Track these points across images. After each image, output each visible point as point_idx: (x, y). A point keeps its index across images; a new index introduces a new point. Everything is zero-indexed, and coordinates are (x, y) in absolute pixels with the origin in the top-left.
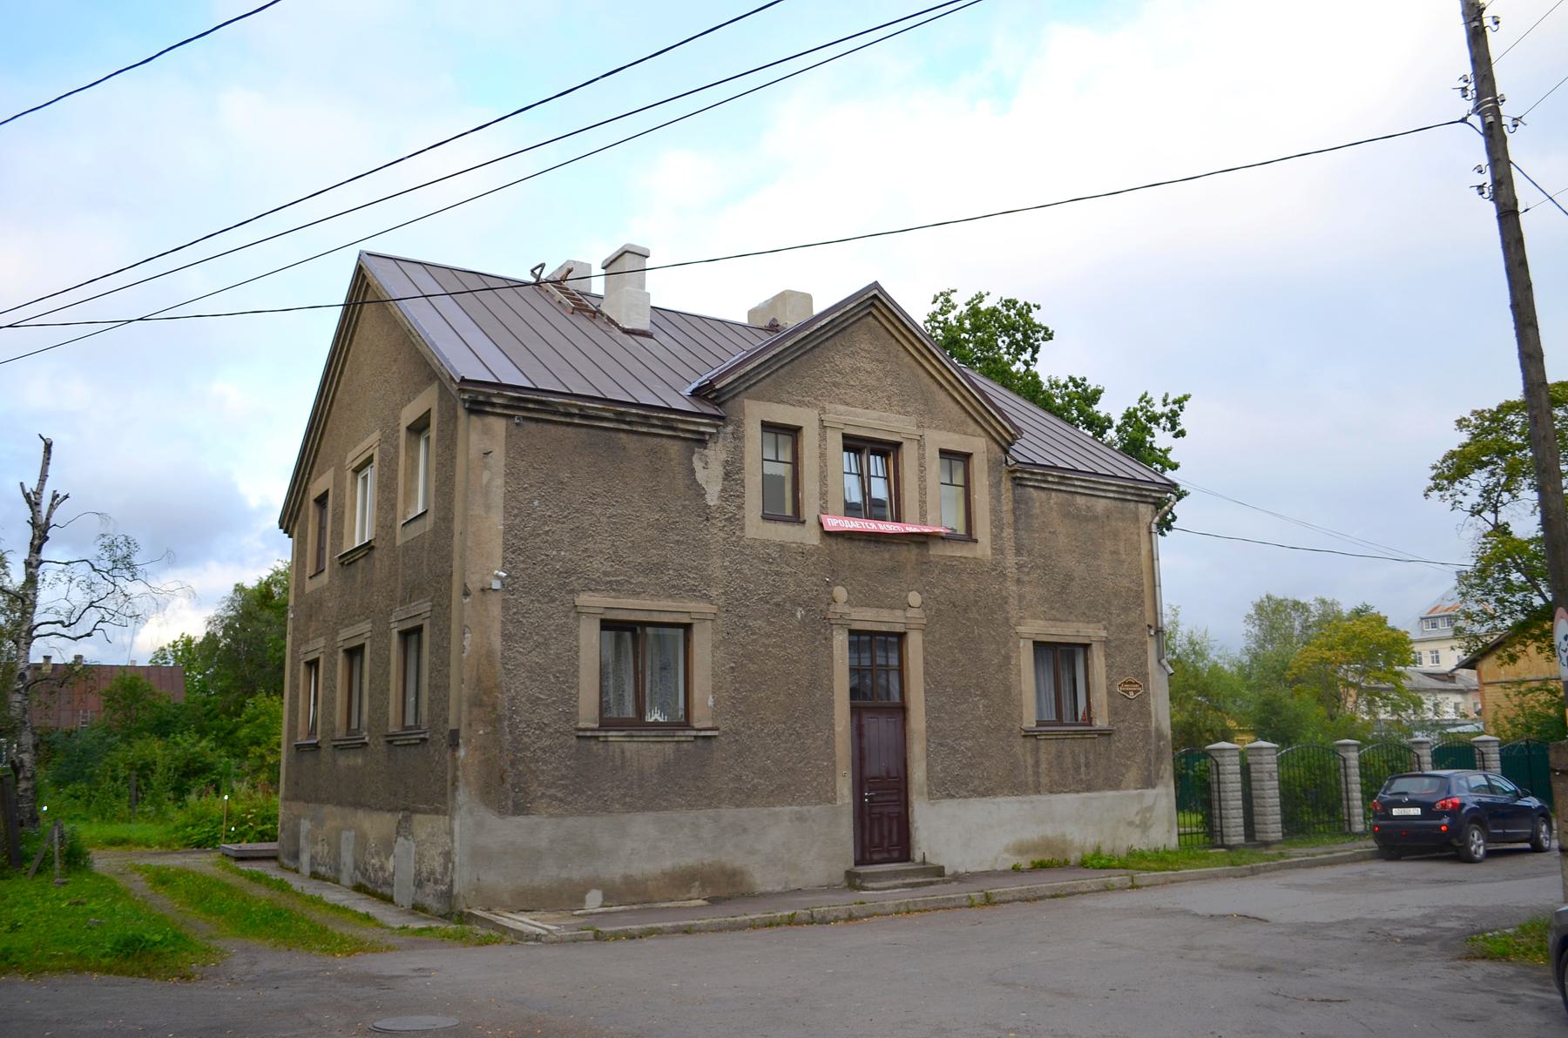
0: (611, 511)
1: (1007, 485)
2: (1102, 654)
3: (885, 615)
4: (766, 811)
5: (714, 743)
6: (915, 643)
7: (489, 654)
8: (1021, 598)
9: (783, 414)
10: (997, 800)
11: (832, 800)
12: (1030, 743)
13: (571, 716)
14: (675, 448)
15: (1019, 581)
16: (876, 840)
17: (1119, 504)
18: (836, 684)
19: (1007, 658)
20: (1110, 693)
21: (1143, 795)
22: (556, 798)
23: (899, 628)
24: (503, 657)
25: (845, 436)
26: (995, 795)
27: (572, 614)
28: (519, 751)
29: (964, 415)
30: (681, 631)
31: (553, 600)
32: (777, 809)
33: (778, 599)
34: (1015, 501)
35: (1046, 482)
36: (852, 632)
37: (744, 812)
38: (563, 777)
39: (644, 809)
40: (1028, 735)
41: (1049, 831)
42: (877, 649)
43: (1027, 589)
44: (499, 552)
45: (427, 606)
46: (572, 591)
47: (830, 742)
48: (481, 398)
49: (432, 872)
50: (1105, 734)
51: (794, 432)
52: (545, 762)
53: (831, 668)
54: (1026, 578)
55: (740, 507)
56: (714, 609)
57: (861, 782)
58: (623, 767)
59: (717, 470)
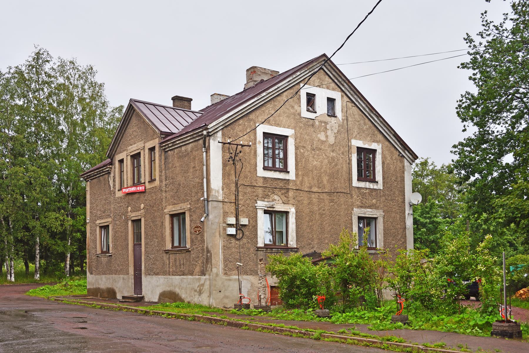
1: (163, 153)
15: (166, 191)
19: (162, 222)
20: (191, 233)
21: (200, 279)
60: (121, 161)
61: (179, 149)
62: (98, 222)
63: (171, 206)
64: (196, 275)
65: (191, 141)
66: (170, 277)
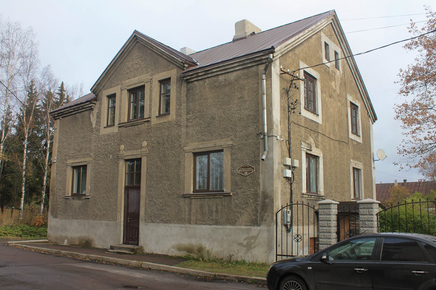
3: (135, 152)
4: (99, 222)
6: (144, 161)
8: (187, 133)
10: (171, 225)
12: (187, 201)
13: (64, 193)
15: (187, 126)
19: (179, 162)
20: (232, 174)
21: (249, 230)
23: (139, 157)
25: (128, 90)
26: (171, 223)
34: (188, 90)
36: (126, 160)
38: (63, 209)
39: (75, 219)
40: (185, 196)
42: (134, 165)
54: (191, 124)
55: (99, 126)
57: (127, 214)
60: (112, 97)
61: (215, 78)
62: (70, 162)
63: (196, 143)
65: (238, 68)
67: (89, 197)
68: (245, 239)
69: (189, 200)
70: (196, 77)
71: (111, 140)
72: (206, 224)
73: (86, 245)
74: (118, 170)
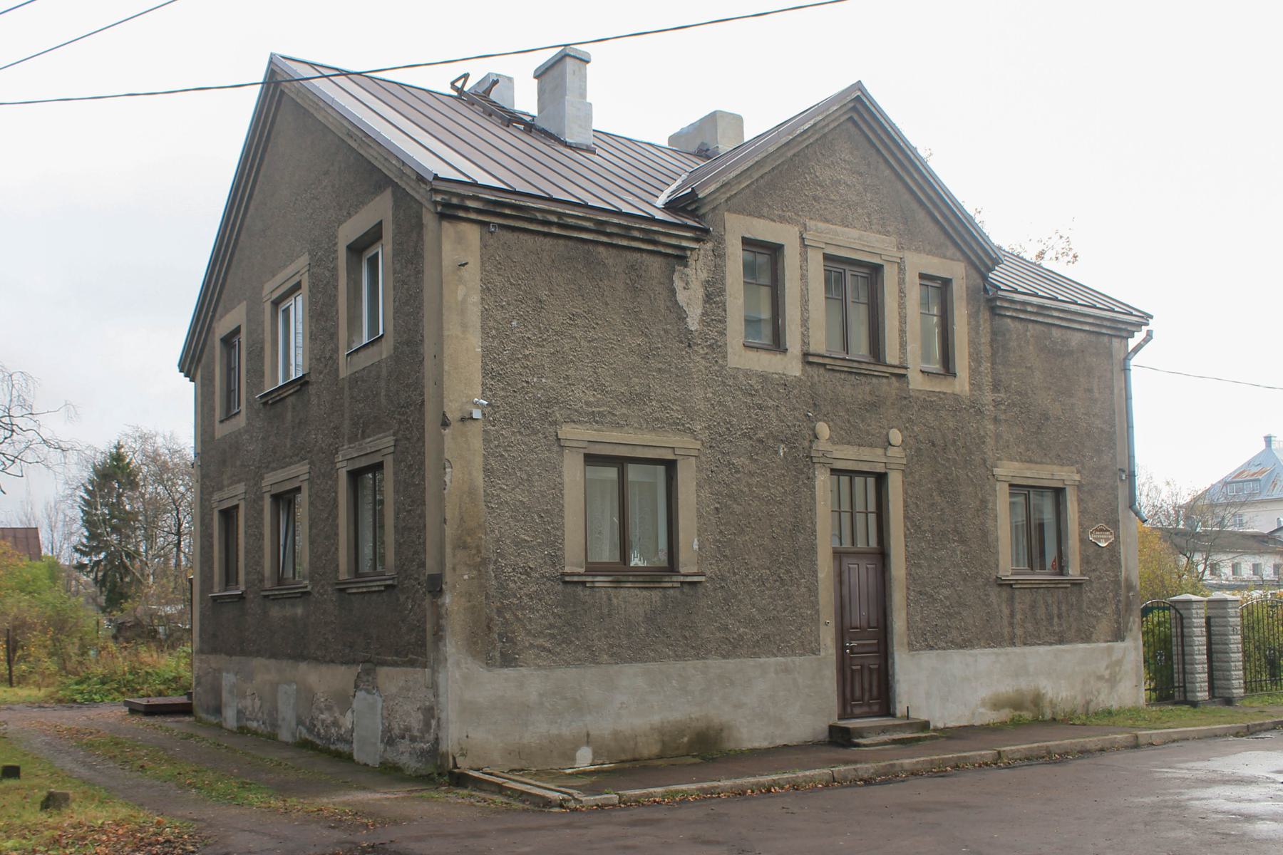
0: (592, 334)
1: (985, 315)
2: (1075, 498)
4: (751, 662)
5: (701, 590)
6: (895, 483)
7: (472, 492)
8: (998, 437)
9: (765, 230)
11: (816, 651)
13: (556, 559)
14: (655, 264)
16: (858, 693)
17: (1093, 338)
18: (819, 527)
19: (984, 502)
21: (1110, 651)
22: (545, 649)
24: (487, 495)
26: (973, 647)
27: (556, 448)
28: (506, 597)
29: (942, 238)
30: (661, 469)
31: (536, 432)
32: (762, 660)
33: (761, 435)
34: (994, 333)
35: (1025, 312)
36: (835, 472)
37: (731, 664)
38: (551, 626)
39: (633, 660)
41: (1025, 684)
43: (1003, 428)
44: (478, 377)
45: (389, 441)
46: (555, 423)
47: (813, 590)
48: (455, 201)
49: (408, 729)
50: (1076, 584)
51: (775, 251)
52: (532, 610)
53: (812, 509)
56: (698, 445)
58: (610, 615)
59: (697, 292)
64: (1098, 641)
66: (1017, 650)
67: (703, 579)
68: (1107, 668)
69: (1009, 589)
70: (1016, 310)
71: (775, 395)
72: (1043, 644)
73: (703, 749)
74: (814, 498)
